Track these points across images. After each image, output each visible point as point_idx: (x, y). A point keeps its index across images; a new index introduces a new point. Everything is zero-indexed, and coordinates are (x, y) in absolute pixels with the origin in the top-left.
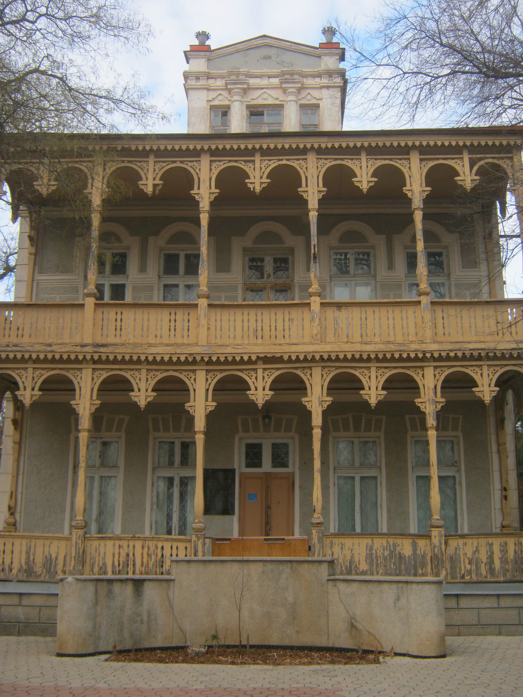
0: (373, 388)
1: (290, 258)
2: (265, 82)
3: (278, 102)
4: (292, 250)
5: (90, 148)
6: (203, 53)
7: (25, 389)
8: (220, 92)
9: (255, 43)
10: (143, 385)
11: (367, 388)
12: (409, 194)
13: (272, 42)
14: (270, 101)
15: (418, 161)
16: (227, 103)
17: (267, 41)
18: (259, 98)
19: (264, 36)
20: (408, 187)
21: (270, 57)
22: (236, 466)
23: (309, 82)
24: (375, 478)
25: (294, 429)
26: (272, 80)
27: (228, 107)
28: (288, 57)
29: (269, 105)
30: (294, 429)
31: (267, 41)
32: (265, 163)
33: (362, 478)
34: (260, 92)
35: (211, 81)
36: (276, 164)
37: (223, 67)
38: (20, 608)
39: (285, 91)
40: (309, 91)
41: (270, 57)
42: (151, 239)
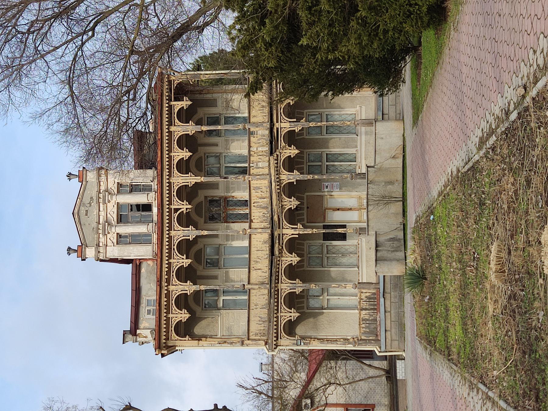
0: (290, 151)
1: (209, 199)
2: (102, 214)
3: (116, 206)
4: (206, 197)
5: (166, 292)
6: (83, 249)
7: (291, 316)
8: (108, 240)
9: (77, 219)
10: (290, 259)
11: (290, 154)
12: (193, 132)
13: (76, 209)
14: (115, 210)
15: (175, 127)
16: (115, 234)
17: (76, 211)
18: (113, 216)
19: (73, 214)
20: (189, 133)
21: (87, 211)
22: (322, 224)
23: (103, 188)
24: (327, 154)
25: (303, 195)
26: (101, 209)
27: (117, 234)
28: (86, 200)
29: (117, 211)
30: (303, 195)
31: (76, 211)
32: (175, 203)
33: (327, 162)
34: (108, 215)
35: (101, 244)
36: (176, 197)
37: (90, 238)
38: (392, 312)
39: (109, 202)
40: (109, 187)
41: (87, 211)
42: (199, 273)
